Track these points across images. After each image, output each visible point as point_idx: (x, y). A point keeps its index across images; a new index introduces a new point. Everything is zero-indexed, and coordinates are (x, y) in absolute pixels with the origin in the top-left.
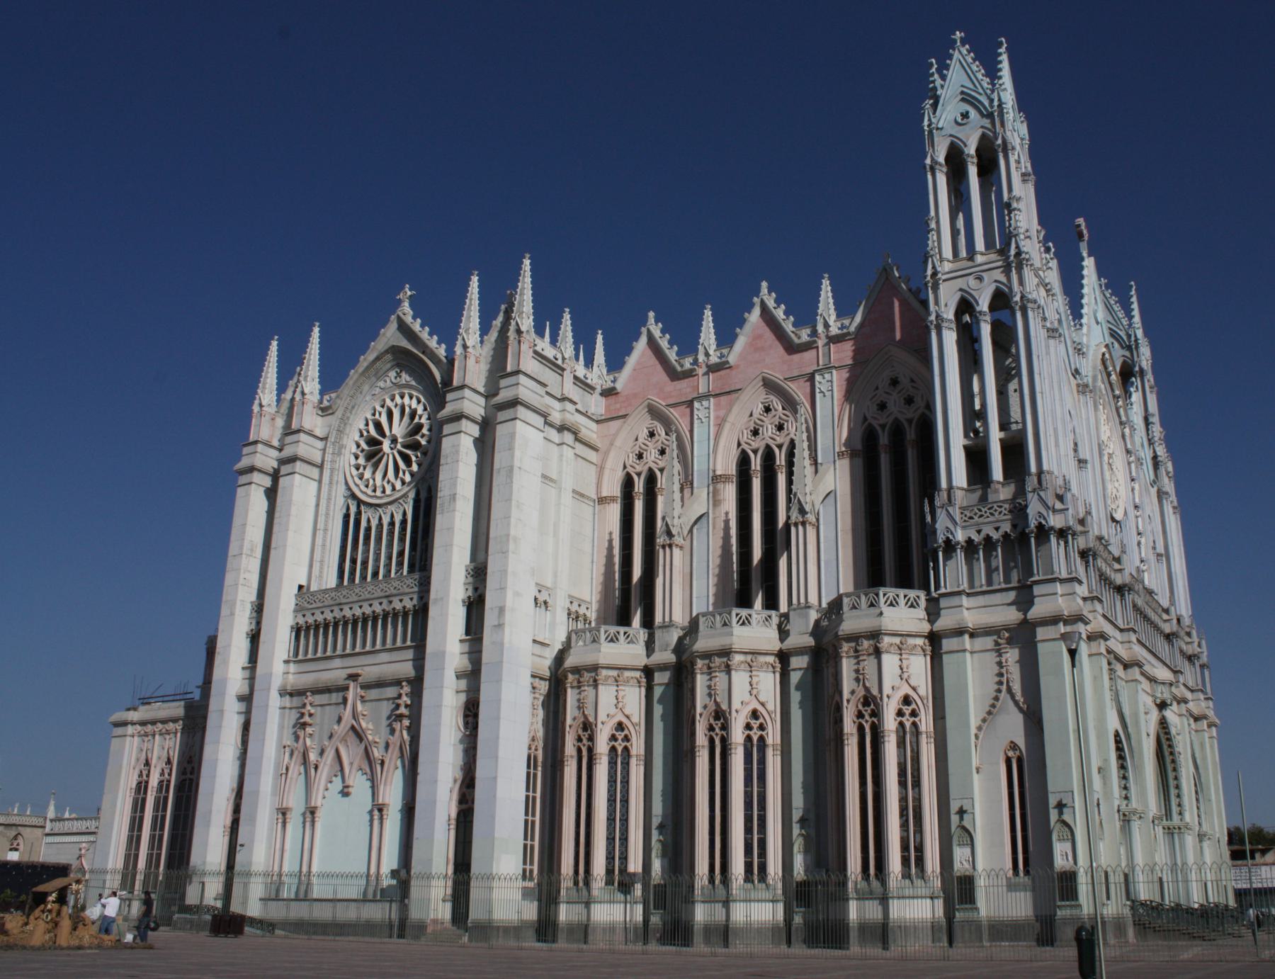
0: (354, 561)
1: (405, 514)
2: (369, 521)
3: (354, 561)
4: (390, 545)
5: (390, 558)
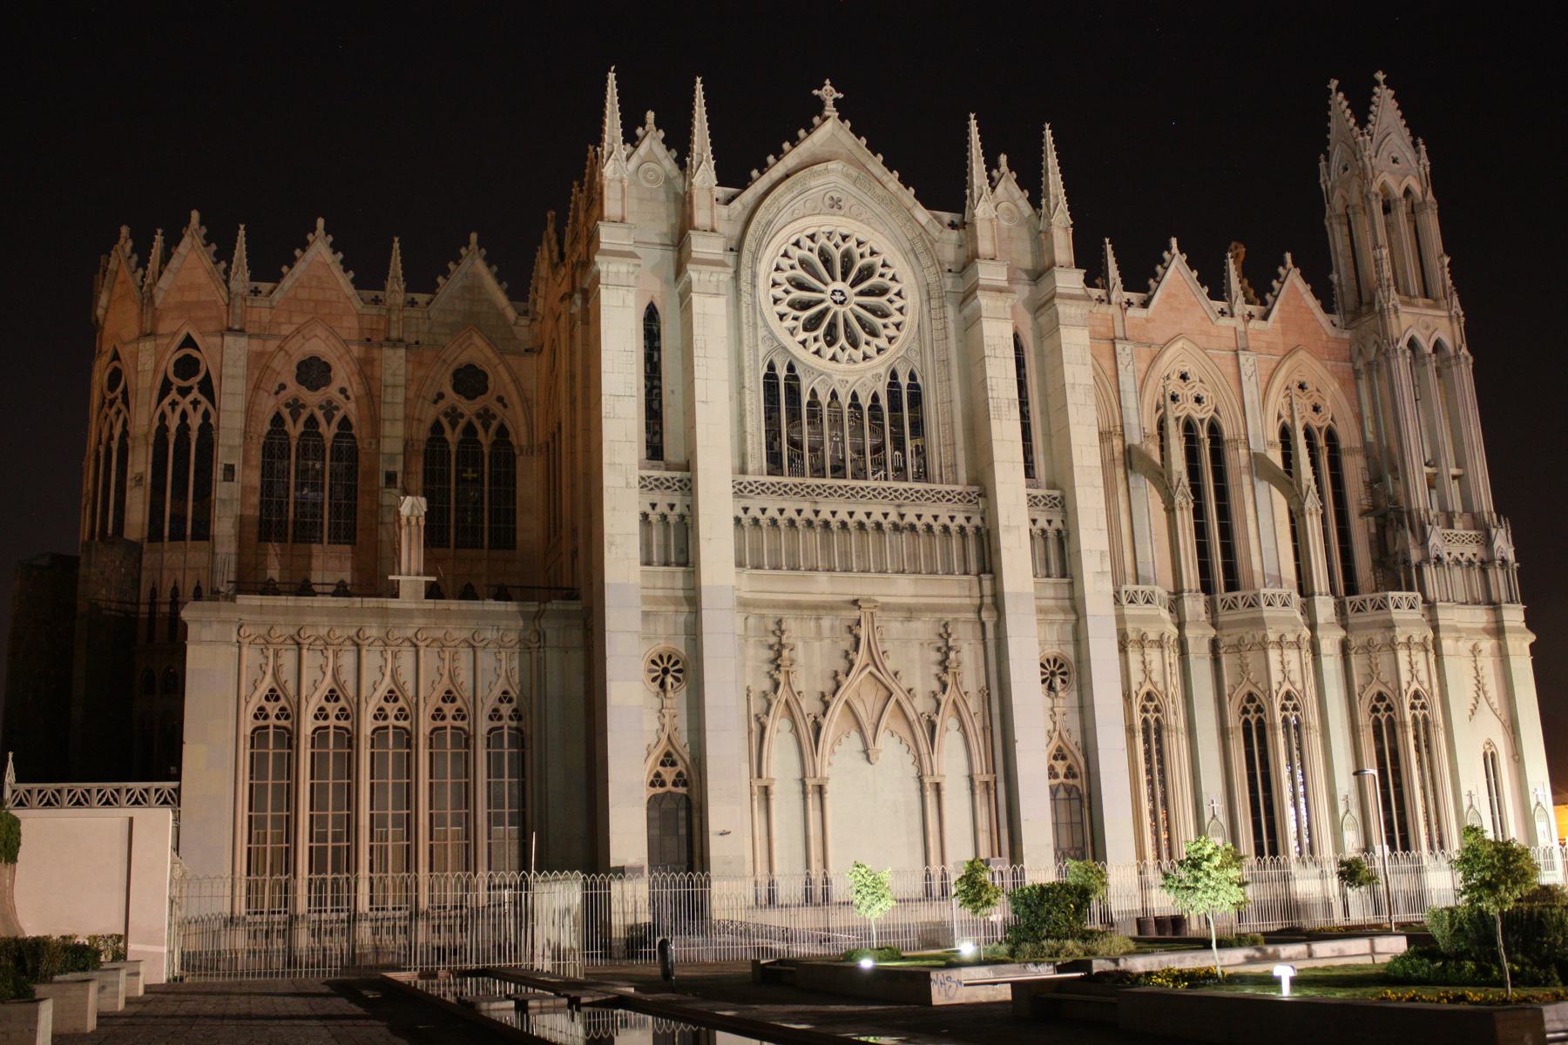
0: (795, 444)
1: (875, 398)
2: (814, 393)
3: (795, 444)
4: (858, 429)
5: (860, 452)
